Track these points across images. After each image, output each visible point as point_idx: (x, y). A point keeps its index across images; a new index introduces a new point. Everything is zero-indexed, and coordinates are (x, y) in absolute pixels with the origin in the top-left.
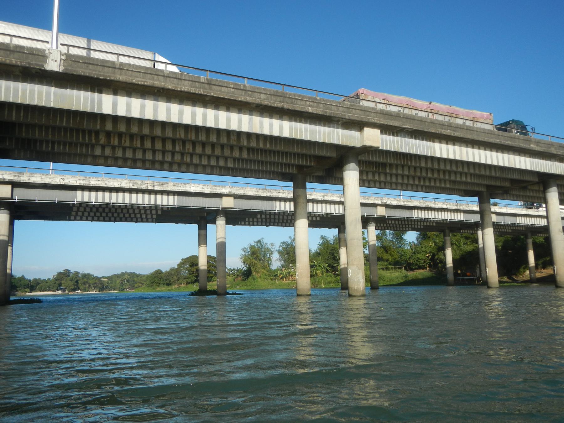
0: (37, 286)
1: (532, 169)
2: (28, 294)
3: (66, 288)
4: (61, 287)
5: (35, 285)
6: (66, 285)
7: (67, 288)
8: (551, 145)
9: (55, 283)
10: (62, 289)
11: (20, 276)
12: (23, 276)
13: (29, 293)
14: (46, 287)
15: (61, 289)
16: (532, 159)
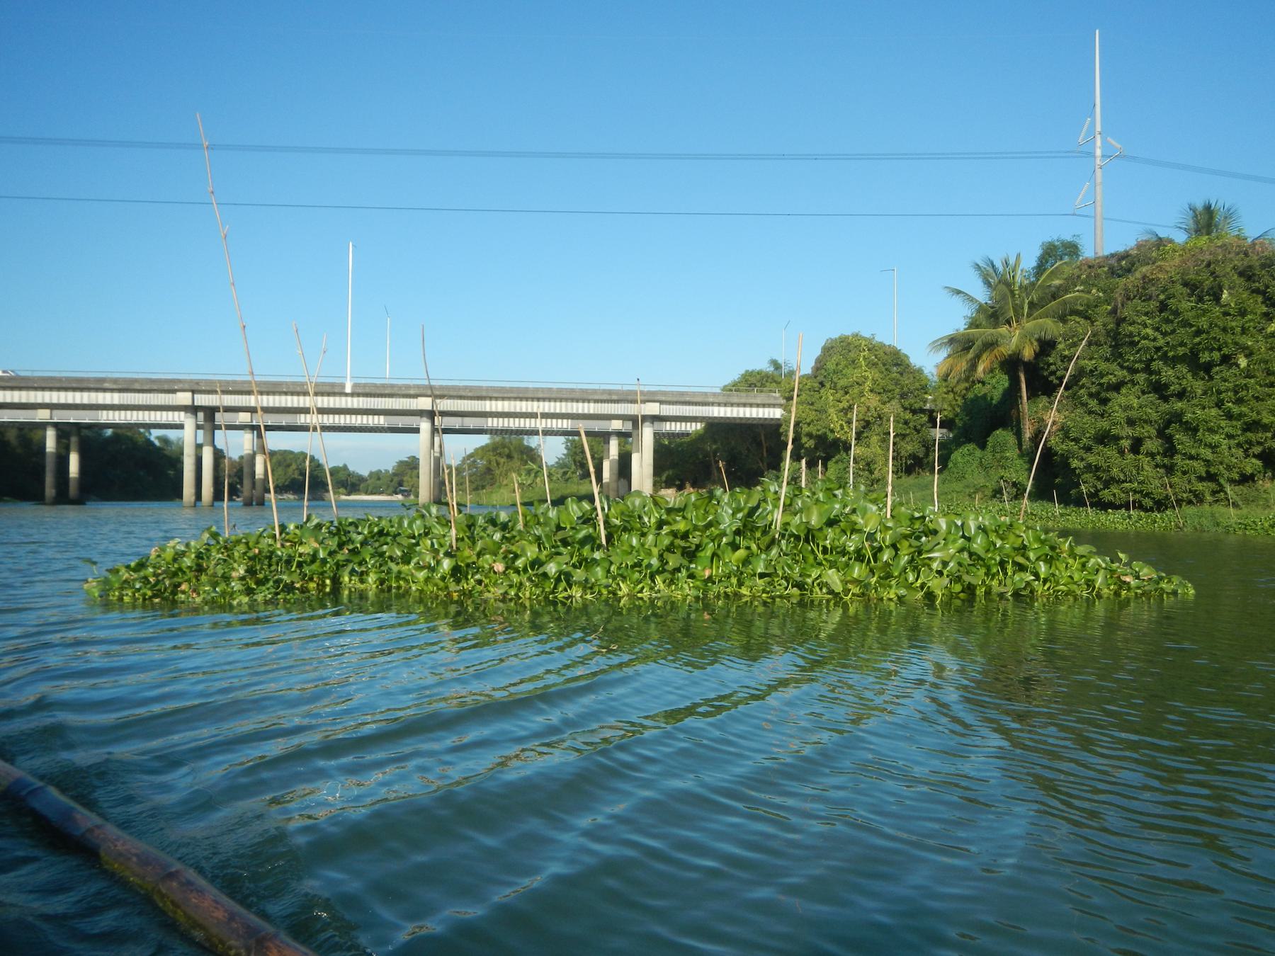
0: (359, 485)
1: (122, 403)
2: (344, 497)
3: (411, 491)
4: (402, 488)
5: (357, 482)
6: (411, 484)
7: (413, 489)
8: (136, 381)
9: (392, 481)
10: (406, 491)
11: (341, 465)
12: (345, 467)
13: (346, 495)
14: (374, 488)
15: (402, 492)
16: (122, 394)
